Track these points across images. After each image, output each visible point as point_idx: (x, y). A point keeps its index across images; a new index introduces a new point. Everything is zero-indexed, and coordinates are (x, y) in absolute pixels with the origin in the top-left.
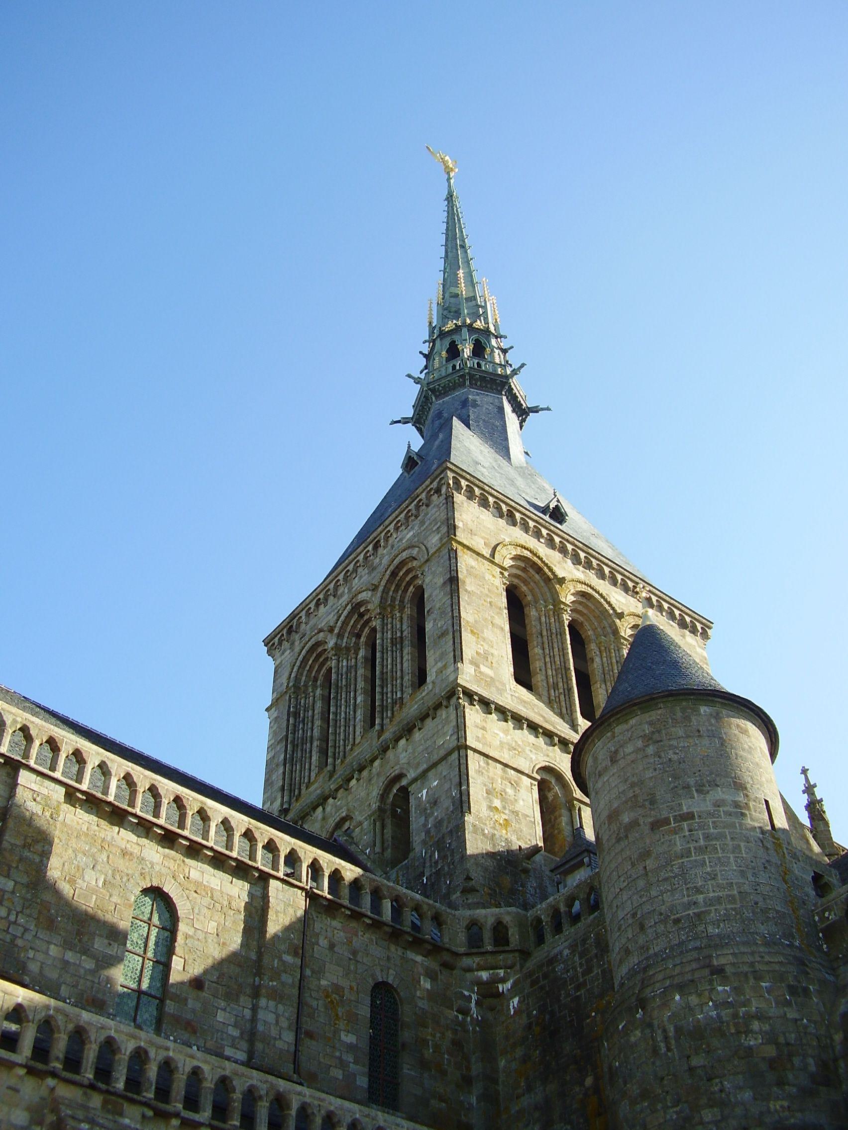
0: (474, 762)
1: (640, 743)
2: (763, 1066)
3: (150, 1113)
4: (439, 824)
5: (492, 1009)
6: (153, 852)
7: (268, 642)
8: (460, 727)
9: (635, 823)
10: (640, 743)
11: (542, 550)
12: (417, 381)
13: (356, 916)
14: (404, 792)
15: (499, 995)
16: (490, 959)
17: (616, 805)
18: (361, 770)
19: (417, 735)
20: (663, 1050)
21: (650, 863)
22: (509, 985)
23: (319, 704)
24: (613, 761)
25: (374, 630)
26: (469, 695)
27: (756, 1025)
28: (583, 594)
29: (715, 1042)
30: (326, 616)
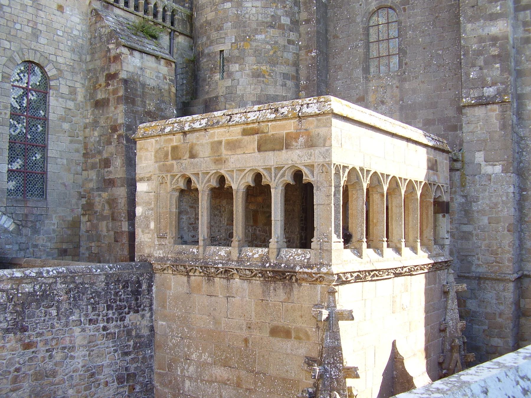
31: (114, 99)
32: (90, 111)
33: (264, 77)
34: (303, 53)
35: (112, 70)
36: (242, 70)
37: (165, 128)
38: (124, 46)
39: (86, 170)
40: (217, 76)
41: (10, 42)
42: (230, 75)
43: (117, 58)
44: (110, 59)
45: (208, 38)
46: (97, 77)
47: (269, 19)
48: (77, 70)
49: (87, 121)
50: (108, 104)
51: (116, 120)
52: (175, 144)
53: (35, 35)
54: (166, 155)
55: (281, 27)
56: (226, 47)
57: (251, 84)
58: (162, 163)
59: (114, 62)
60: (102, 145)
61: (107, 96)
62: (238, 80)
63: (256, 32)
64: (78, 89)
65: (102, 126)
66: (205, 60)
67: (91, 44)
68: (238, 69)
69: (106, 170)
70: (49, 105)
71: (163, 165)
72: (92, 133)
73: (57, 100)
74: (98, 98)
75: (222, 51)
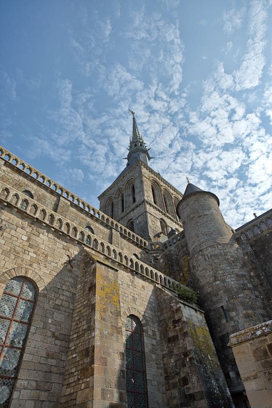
0: (149, 215)
1: (194, 202)
2: (231, 262)
3: (105, 257)
4: (141, 227)
5: (156, 262)
6: (89, 220)
7: (98, 198)
8: (145, 208)
9: (194, 217)
10: (194, 202)
11: (158, 179)
12: (129, 150)
13: (129, 240)
14: (132, 222)
15: (158, 259)
16: (156, 252)
17: (189, 214)
18: (122, 218)
19: (135, 211)
20: (207, 259)
21: (198, 224)
22: (160, 257)
23: (110, 209)
24: (187, 205)
25: (123, 194)
26: (147, 202)
27: (228, 254)
28: (165, 189)
29: (220, 257)
30: (112, 191)
31: (181, 334)
32: (165, 346)
33: (252, 317)
34: (266, 302)
35: (176, 318)
36: (237, 315)
37: (255, 333)
38: (181, 303)
39: (169, 390)
40: (224, 321)
41: (124, 303)
42: (232, 319)
43: (178, 310)
44: (173, 311)
45: (211, 301)
46: (167, 324)
47: (242, 286)
48: (154, 321)
49: (165, 352)
50: (178, 339)
51: (186, 347)
52: (270, 342)
53: (134, 299)
54: (265, 353)
55: (249, 289)
56: (224, 304)
57: (246, 322)
58: (263, 360)
59: (176, 312)
60: (179, 368)
61: (176, 334)
62: (238, 321)
63: (237, 293)
64: (156, 332)
65: (176, 355)
66: (213, 314)
67: (159, 306)
68: (235, 315)
69: (186, 387)
70: (144, 342)
71: (265, 362)
72: (169, 360)
73: (148, 339)
74: (169, 336)
75: (222, 307)
